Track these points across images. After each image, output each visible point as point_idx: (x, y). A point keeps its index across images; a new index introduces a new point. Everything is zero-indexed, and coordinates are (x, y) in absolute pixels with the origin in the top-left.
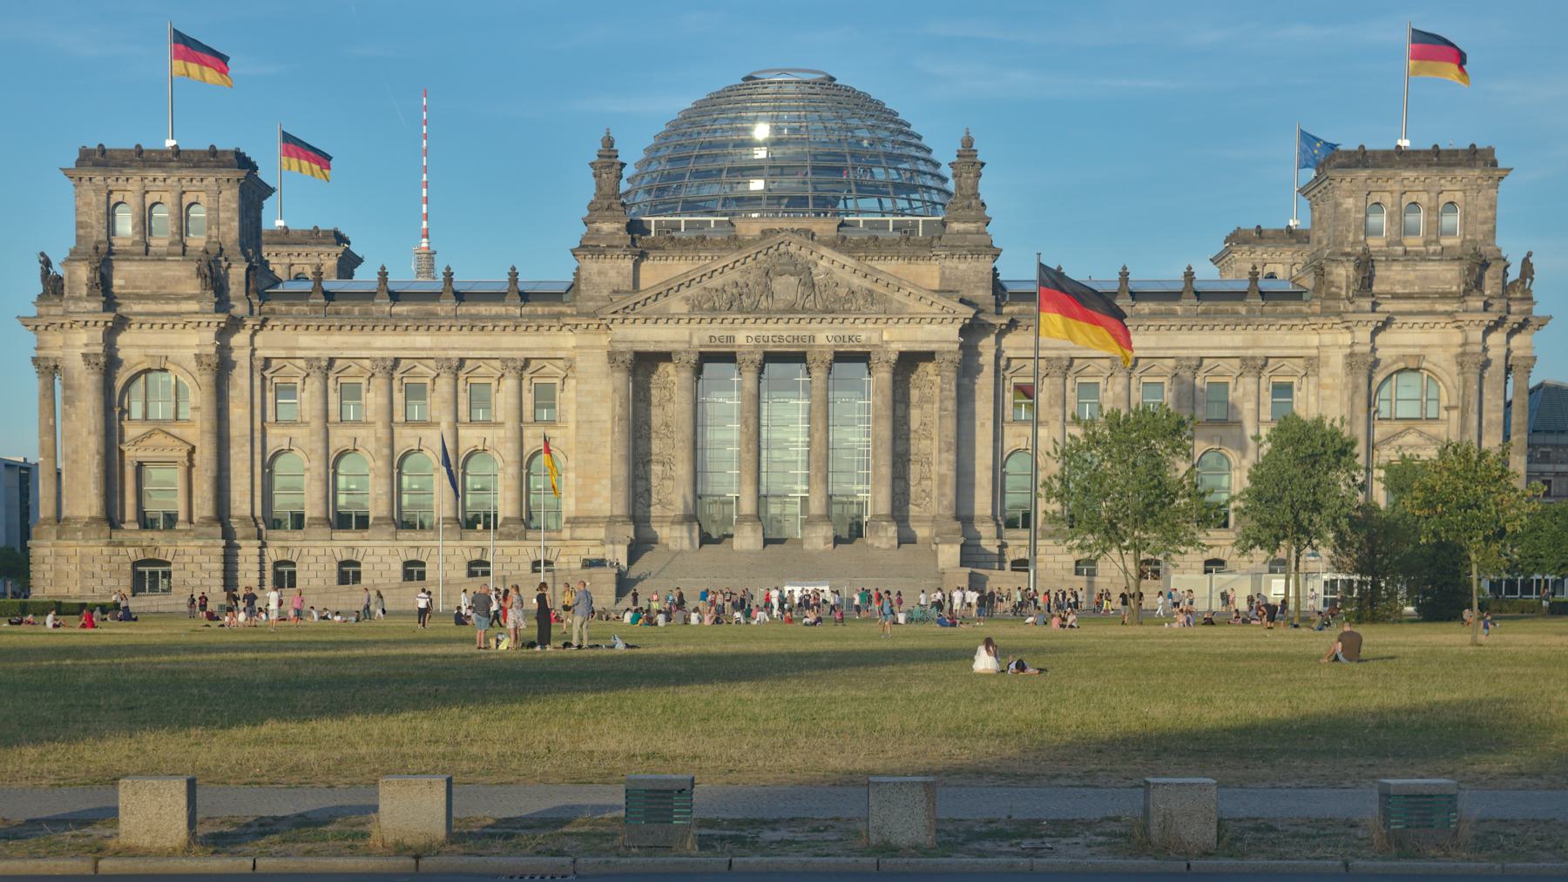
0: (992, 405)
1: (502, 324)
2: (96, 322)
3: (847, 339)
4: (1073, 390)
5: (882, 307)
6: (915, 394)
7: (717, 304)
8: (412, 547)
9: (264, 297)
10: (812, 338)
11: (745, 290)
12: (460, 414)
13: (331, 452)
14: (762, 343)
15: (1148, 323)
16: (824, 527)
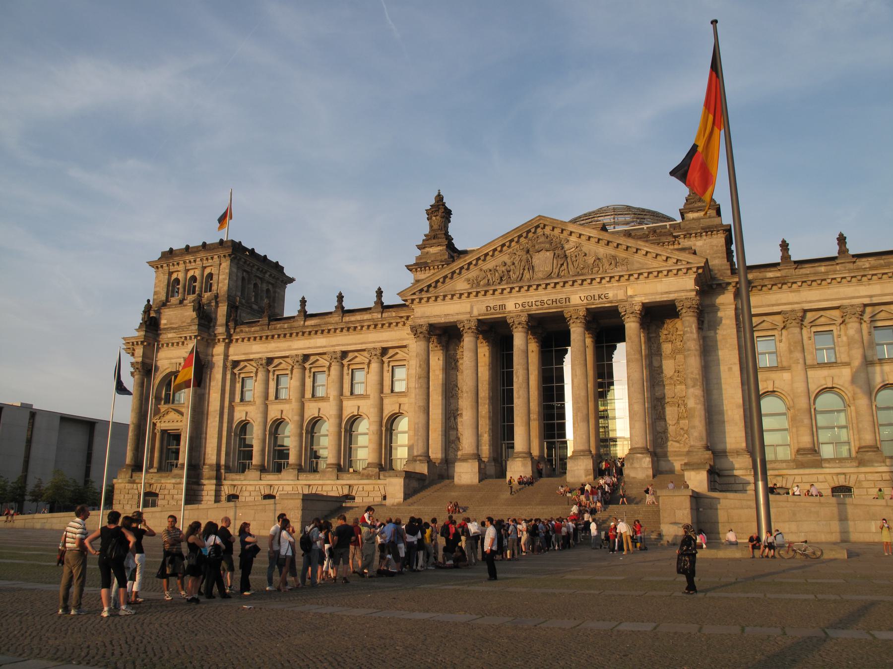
0: (737, 352)
1: (365, 324)
2: (137, 342)
3: (597, 297)
4: (810, 338)
5: (625, 268)
6: (667, 348)
7: (491, 281)
8: (306, 485)
9: (237, 324)
10: (568, 300)
11: (512, 267)
12: (344, 391)
13: (268, 420)
14: (527, 307)
15: (871, 272)
16: (585, 460)
